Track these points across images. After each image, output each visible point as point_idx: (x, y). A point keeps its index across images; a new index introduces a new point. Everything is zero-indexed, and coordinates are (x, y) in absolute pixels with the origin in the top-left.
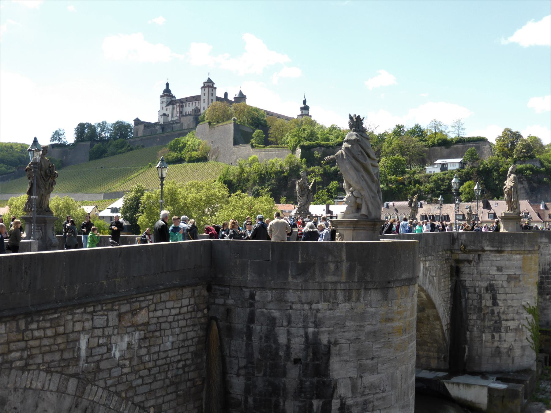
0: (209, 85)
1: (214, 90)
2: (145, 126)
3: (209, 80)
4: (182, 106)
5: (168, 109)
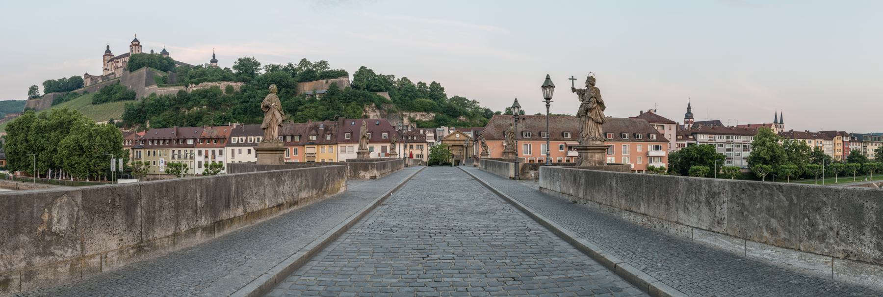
0: (136, 43)
2: (92, 79)
3: (136, 40)
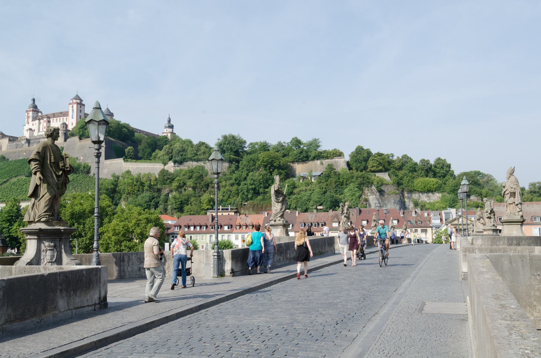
1: (82, 106)
4: (49, 122)
5: (34, 124)
